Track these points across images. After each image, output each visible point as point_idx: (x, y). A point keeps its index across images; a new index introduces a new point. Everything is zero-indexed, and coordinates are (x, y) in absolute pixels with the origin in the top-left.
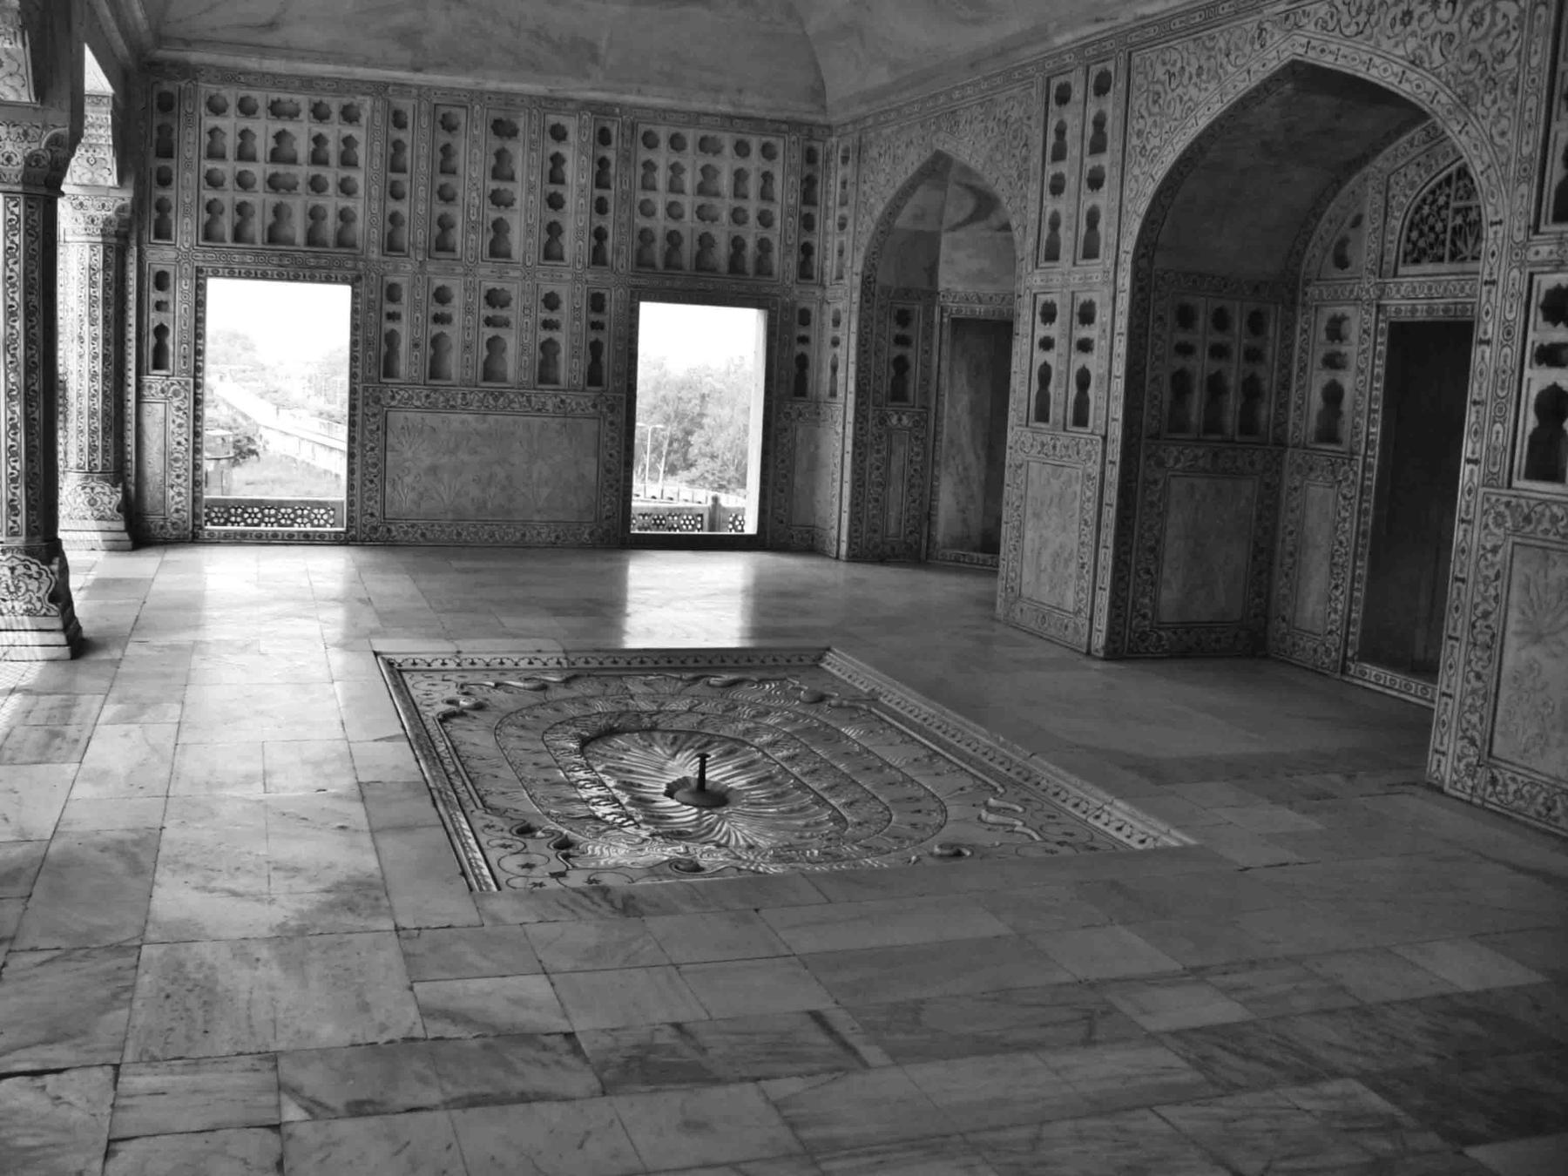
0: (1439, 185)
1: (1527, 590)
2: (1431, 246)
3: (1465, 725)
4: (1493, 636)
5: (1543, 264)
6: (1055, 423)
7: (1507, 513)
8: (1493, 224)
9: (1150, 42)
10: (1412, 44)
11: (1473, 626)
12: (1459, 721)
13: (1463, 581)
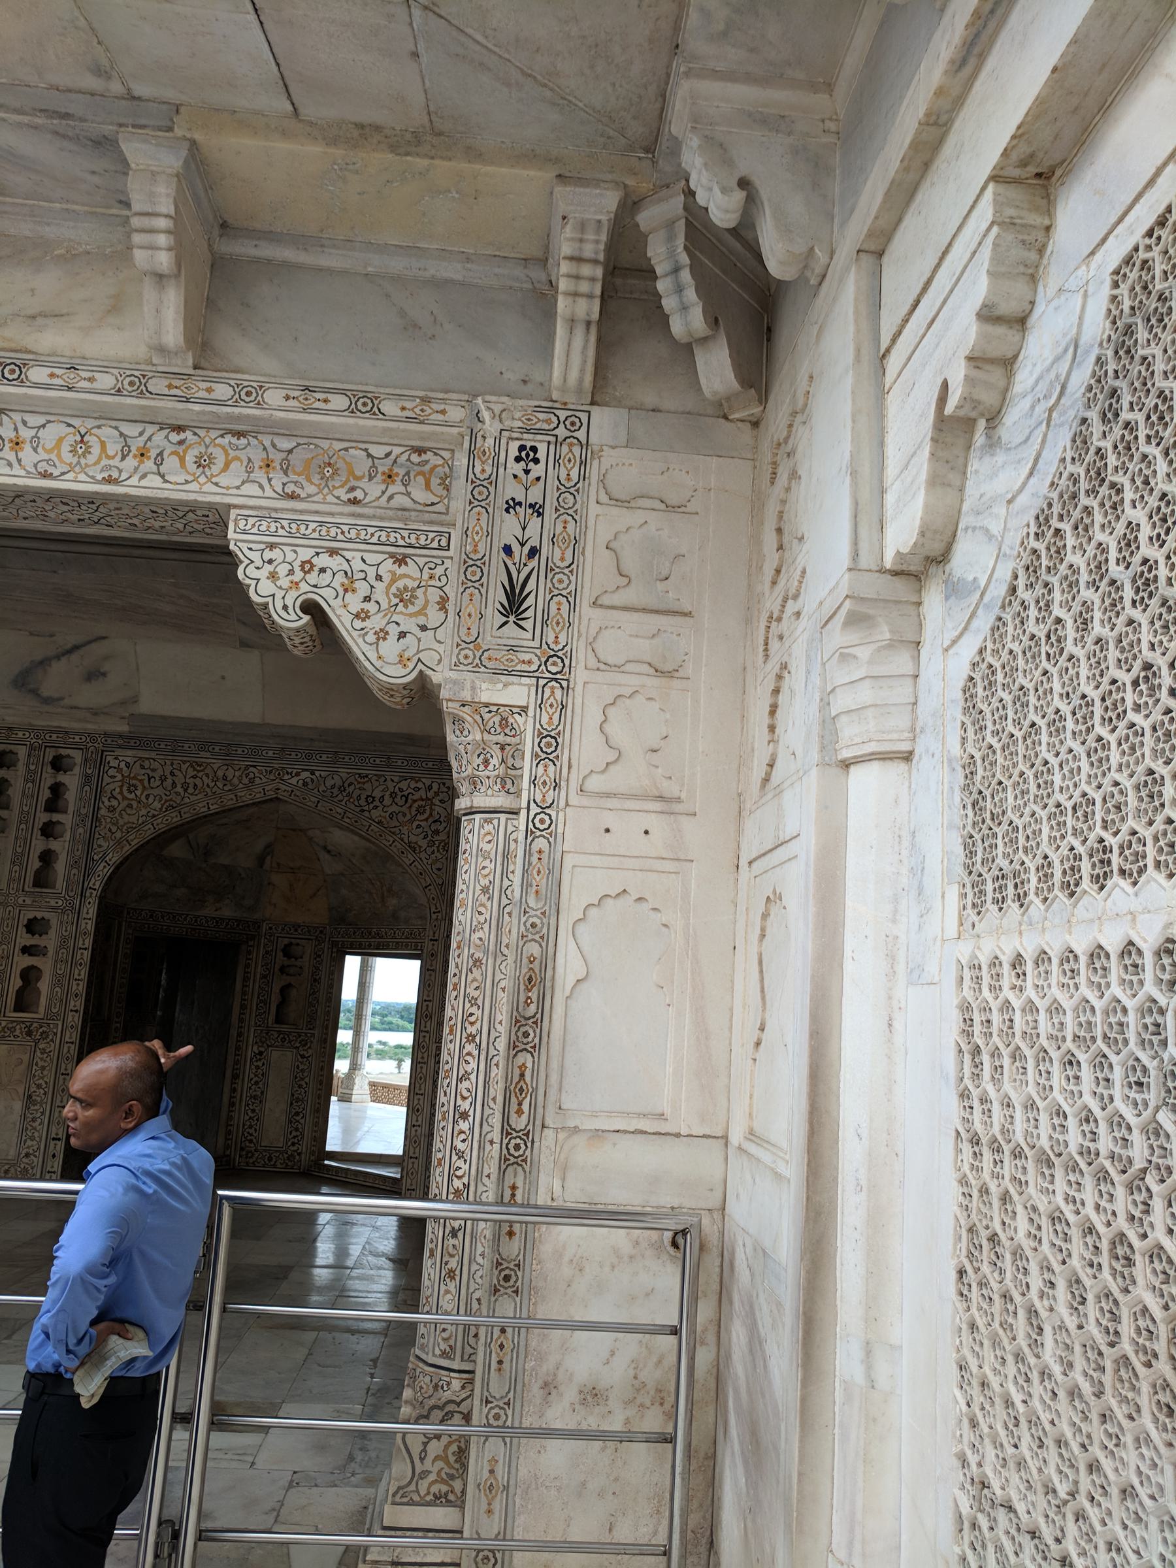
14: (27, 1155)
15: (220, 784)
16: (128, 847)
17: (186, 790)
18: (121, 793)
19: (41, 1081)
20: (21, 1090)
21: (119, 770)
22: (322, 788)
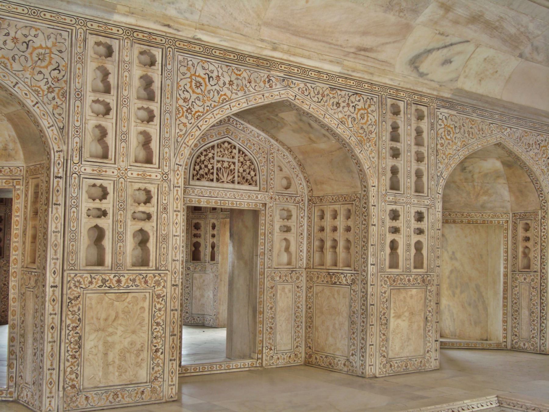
0: (209, 148)
1: (395, 303)
2: (206, 174)
4: (387, 320)
5: (391, 202)
6: (117, 266)
7: (388, 280)
8: (373, 186)
10: (341, 115)
11: (381, 319)
12: (379, 351)
13: (373, 305)
14: (428, 352)
15: (481, 133)
16: (450, 169)
17: (469, 135)
18: (445, 135)
19: (430, 309)
20: (423, 316)
21: (443, 122)
22: (514, 138)
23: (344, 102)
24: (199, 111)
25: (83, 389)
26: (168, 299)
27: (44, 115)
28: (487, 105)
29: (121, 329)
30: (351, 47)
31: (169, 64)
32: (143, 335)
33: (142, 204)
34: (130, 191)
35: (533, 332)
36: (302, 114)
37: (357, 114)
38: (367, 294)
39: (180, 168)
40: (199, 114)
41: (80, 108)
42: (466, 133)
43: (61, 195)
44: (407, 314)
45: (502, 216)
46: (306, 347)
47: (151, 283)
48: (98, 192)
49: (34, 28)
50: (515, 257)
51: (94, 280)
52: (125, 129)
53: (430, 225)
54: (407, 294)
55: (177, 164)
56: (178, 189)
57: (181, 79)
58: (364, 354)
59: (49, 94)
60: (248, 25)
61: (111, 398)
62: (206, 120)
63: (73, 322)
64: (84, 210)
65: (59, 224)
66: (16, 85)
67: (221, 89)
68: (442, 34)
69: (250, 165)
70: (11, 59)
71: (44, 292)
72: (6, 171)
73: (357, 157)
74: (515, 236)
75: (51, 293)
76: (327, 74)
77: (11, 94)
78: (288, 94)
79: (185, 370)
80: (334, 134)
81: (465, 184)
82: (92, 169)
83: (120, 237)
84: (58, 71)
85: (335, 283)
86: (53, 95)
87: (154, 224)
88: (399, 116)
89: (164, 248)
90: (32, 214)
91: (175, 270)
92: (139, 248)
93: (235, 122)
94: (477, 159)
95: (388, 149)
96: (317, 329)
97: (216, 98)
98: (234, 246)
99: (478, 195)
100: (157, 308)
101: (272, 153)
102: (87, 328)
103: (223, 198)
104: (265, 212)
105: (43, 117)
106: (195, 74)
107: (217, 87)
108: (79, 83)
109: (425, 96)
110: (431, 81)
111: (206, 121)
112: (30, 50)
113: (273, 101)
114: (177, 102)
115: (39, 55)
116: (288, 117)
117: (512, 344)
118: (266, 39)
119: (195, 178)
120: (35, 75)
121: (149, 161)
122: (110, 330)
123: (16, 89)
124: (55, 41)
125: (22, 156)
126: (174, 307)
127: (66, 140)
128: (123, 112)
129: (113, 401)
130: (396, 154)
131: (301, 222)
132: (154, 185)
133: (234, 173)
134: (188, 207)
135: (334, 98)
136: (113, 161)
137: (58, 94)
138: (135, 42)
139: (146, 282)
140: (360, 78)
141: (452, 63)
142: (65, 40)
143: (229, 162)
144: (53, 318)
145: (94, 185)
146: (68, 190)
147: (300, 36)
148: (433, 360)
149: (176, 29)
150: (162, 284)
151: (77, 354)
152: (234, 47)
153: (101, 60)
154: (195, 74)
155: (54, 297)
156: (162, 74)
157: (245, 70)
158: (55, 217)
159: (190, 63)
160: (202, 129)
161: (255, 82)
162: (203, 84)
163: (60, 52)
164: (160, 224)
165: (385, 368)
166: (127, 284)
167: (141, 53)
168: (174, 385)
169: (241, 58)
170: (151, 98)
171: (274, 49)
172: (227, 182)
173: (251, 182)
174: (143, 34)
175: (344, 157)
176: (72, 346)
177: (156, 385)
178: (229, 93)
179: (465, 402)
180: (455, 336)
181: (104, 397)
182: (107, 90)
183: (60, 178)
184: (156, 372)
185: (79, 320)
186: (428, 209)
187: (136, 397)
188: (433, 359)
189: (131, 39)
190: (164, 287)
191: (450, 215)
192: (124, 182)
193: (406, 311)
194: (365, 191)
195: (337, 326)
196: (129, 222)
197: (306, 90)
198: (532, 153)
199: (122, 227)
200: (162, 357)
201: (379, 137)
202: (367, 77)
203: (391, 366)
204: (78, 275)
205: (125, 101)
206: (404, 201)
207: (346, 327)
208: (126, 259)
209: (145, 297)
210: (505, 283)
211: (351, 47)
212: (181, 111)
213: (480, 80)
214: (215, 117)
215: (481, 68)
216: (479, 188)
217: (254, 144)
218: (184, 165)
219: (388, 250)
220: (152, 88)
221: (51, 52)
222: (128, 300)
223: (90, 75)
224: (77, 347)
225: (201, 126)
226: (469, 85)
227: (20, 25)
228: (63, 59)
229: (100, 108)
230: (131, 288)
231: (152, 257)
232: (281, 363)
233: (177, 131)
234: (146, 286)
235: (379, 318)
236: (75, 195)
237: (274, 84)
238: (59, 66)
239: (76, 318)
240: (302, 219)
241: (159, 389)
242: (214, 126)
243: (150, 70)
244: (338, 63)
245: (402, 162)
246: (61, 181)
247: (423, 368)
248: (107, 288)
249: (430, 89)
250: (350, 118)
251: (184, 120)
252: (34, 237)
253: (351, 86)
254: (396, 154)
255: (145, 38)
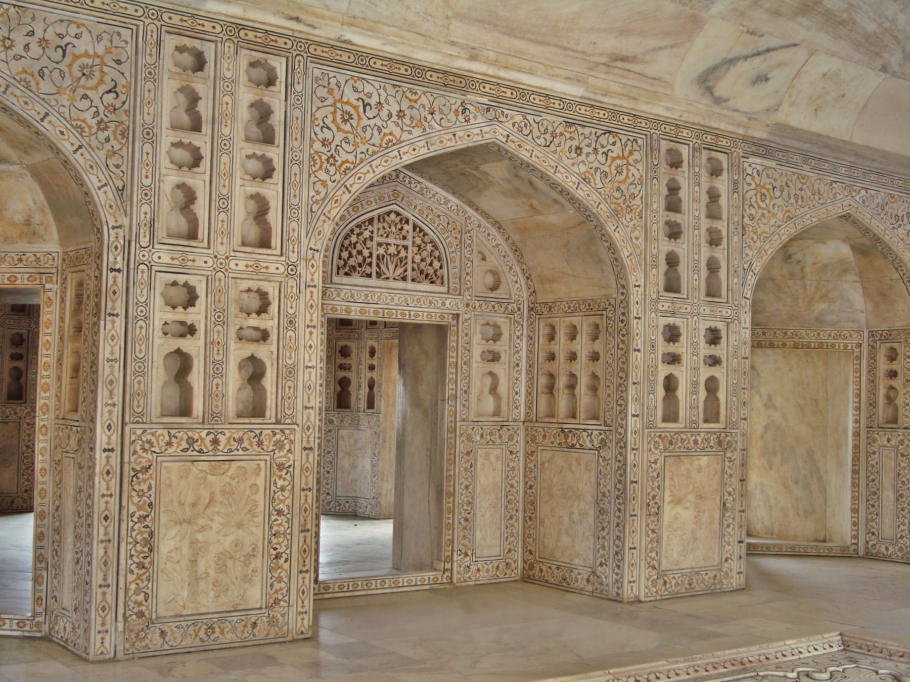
0: (364, 223)
1: (672, 479)
2: (360, 265)
3: (649, 560)
5: (665, 312)
6: (212, 417)
8: (636, 286)
9: (341, 65)
10: (583, 168)
11: (648, 505)
12: (646, 559)
13: (636, 482)
14: (726, 560)
15: (817, 197)
16: (765, 257)
17: (797, 202)
18: (756, 201)
19: (730, 489)
21: (753, 179)
22: (872, 206)
23: (588, 146)
24: (347, 161)
25: (157, 618)
26: (297, 472)
27: (91, 167)
28: (826, 152)
29: (218, 519)
30: (601, 54)
31: (298, 83)
32: (254, 530)
33: (254, 315)
34: (233, 294)
35: (902, 527)
36: (518, 166)
37: (610, 166)
38: (625, 464)
39: (317, 255)
40: (348, 165)
41: (150, 156)
42: (792, 197)
43: (119, 300)
44: (691, 497)
45: (851, 336)
46: (524, 553)
47: (268, 445)
48: (180, 295)
49: (75, 23)
50: (873, 404)
51: (174, 440)
52: (224, 191)
53: (731, 349)
54: (691, 464)
55: (311, 249)
56: (313, 289)
57: (318, 108)
58: (620, 564)
59: (100, 133)
60: (429, 18)
61: (202, 634)
62: (360, 175)
63: (140, 508)
64: (158, 325)
65: (117, 348)
66: (44, 117)
67: (385, 125)
68: (752, 33)
69: (432, 251)
70: (36, 74)
71: (92, 459)
72: (30, 259)
73: (610, 237)
74: (872, 370)
75: (104, 461)
76: (561, 99)
77: (37, 133)
78: (495, 132)
79: (324, 588)
80: (573, 200)
81: (790, 282)
82: (170, 256)
83: (218, 369)
84: (114, 95)
85: (573, 446)
86: (106, 133)
87: (274, 348)
88: (680, 169)
89: (290, 387)
90: (72, 330)
91: (308, 423)
92: (249, 387)
93: (407, 180)
94: (810, 242)
95: (662, 224)
96: (542, 522)
97: (377, 139)
98: (405, 385)
99: (812, 300)
100: (279, 486)
101: (469, 231)
102: (163, 519)
103: (387, 304)
104: (458, 329)
105: (91, 170)
106: (340, 100)
107: (377, 121)
108: (149, 114)
109: (724, 137)
110: (735, 110)
111: (359, 178)
112: (68, 60)
113: (470, 145)
114: (311, 146)
115: (83, 67)
116: (496, 170)
117: (867, 548)
118: (460, 41)
119: (341, 271)
120: (76, 100)
121: (264, 243)
122: (201, 522)
123: (45, 124)
124: (109, 44)
125: (55, 235)
126: (307, 484)
127: (128, 209)
128: (222, 162)
129: (206, 638)
130: (674, 232)
131: (516, 346)
132: (273, 284)
133: (406, 263)
134: (330, 321)
135: (572, 139)
136: (205, 244)
137: (114, 132)
138: (241, 47)
139: (260, 444)
140: (615, 105)
141: (770, 82)
142: (126, 42)
143: (398, 246)
144: (107, 503)
145: (175, 284)
146: (131, 290)
147: (516, 37)
148: (734, 573)
149: (309, 25)
150: (287, 447)
151: (147, 561)
152: (405, 54)
153: (185, 77)
154: (340, 100)
155: (108, 467)
156: (286, 100)
157: (424, 93)
158: (110, 335)
159: (333, 81)
160: (353, 190)
161: (441, 112)
162: (355, 116)
163: (119, 62)
164: (284, 347)
165: (655, 586)
166: (228, 447)
167: (252, 65)
168: (306, 612)
169: (417, 73)
170: (268, 139)
171: (473, 58)
172: (394, 279)
173: (435, 279)
174: (255, 33)
175: (589, 238)
176: (139, 548)
177: (277, 612)
178: (397, 131)
179: (788, 642)
180: (772, 534)
181: (190, 631)
182: (196, 127)
183: (119, 271)
184: (276, 592)
185: (150, 505)
186: (728, 324)
187: (243, 632)
188: (735, 572)
189: (236, 41)
190: (289, 451)
191: (764, 333)
192: (223, 278)
193: (690, 493)
194: (622, 294)
195: (576, 517)
196: (233, 345)
197: (526, 125)
198: (901, 231)
199: (221, 352)
200: (286, 566)
201: (647, 205)
202: (627, 104)
203: (665, 583)
204: (149, 431)
205: (225, 145)
206: (689, 310)
207: (591, 519)
208: (227, 407)
209: (260, 470)
210: (856, 447)
211: (601, 54)
212: (318, 162)
213: (816, 110)
214: (374, 172)
215: (818, 89)
216: (813, 289)
217: (439, 216)
218: (323, 250)
219: (661, 392)
220: (269, 122)
221: (103, 64)
222: (230, 473)
223: (168, 101)
224: (146, 549)
225: (351, 186)
226: (797, 118)
227: (52, 18)
228: (122, 74)
229: (184, 155)
230: (235, 452)
231: (270, 402)
232: (483, 577)
233: (312, 193)
234: (259, 449)
235: (645, 504)
236: (142, 300)
237: (472, 116)
238: (116, 86)
239: (145, 501)
240: (519, 341)
241: (281, 619)
242: (372, 185)
243: (267, 93)
244: (578, 81)
245: (685, 246)
246: (120, 276)
247: (718, 587)
248: (195, 453)
249: (733, 124)
250: (598, 174)
251: (323, 176)
252: (76, 369)
253: (600, 119)
254: (674, 232)
255: (258, 40)
